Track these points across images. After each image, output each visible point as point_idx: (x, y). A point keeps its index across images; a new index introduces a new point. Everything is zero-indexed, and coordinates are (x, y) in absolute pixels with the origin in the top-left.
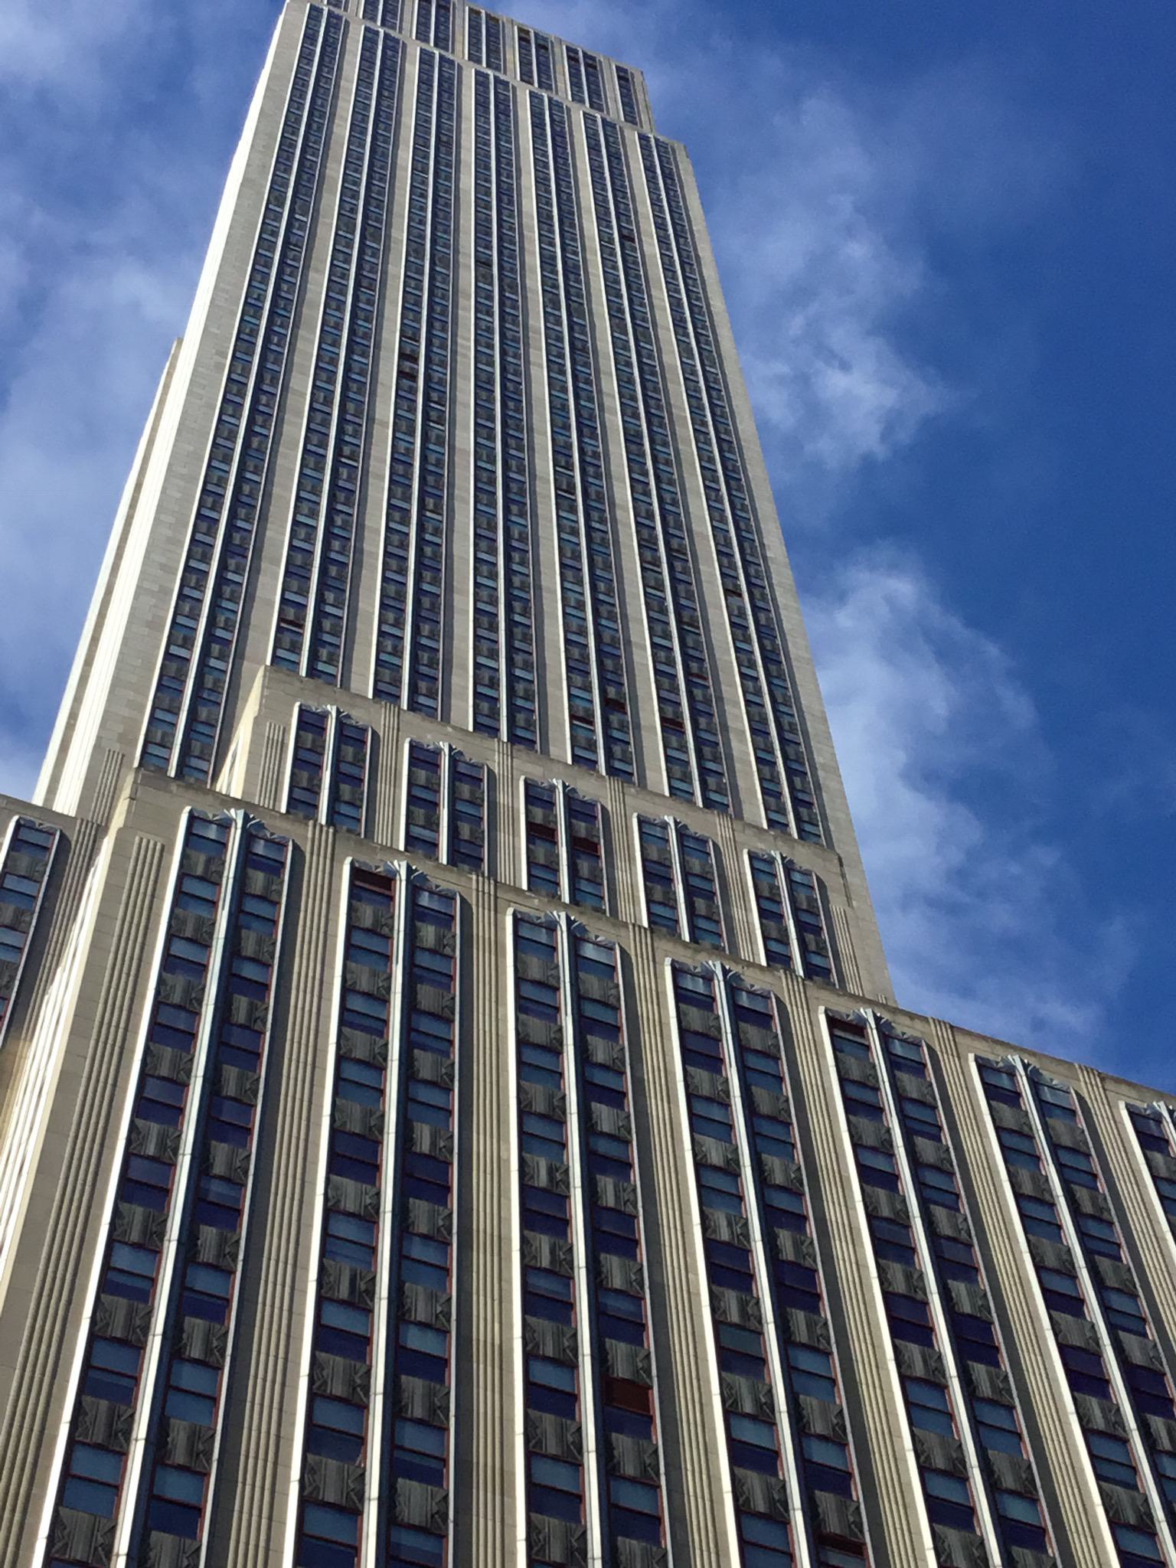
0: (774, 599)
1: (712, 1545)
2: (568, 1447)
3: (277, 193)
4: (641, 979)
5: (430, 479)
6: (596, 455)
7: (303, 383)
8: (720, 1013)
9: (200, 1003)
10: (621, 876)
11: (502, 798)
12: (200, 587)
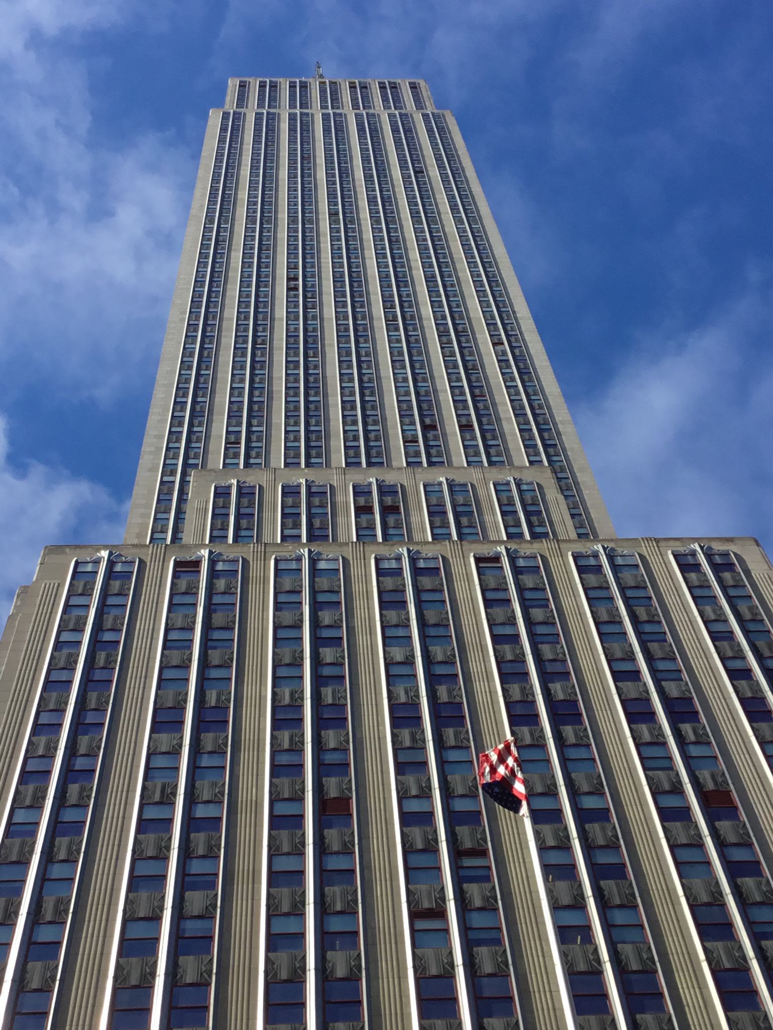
0: (524, 340)
1: (388, 876)
2: (296, 845)
3: (292, 218)
4: (355, 571)
5: (310, 340)
6: (408, 295)
7: (231, 313)
8: (405, 576)
9: (76, 664)
10: (414, 519)
11: (339, 498)
12: (178, 440)
